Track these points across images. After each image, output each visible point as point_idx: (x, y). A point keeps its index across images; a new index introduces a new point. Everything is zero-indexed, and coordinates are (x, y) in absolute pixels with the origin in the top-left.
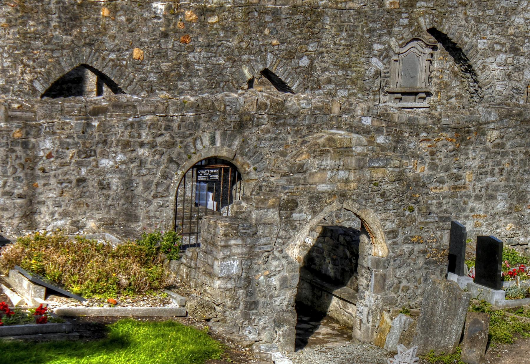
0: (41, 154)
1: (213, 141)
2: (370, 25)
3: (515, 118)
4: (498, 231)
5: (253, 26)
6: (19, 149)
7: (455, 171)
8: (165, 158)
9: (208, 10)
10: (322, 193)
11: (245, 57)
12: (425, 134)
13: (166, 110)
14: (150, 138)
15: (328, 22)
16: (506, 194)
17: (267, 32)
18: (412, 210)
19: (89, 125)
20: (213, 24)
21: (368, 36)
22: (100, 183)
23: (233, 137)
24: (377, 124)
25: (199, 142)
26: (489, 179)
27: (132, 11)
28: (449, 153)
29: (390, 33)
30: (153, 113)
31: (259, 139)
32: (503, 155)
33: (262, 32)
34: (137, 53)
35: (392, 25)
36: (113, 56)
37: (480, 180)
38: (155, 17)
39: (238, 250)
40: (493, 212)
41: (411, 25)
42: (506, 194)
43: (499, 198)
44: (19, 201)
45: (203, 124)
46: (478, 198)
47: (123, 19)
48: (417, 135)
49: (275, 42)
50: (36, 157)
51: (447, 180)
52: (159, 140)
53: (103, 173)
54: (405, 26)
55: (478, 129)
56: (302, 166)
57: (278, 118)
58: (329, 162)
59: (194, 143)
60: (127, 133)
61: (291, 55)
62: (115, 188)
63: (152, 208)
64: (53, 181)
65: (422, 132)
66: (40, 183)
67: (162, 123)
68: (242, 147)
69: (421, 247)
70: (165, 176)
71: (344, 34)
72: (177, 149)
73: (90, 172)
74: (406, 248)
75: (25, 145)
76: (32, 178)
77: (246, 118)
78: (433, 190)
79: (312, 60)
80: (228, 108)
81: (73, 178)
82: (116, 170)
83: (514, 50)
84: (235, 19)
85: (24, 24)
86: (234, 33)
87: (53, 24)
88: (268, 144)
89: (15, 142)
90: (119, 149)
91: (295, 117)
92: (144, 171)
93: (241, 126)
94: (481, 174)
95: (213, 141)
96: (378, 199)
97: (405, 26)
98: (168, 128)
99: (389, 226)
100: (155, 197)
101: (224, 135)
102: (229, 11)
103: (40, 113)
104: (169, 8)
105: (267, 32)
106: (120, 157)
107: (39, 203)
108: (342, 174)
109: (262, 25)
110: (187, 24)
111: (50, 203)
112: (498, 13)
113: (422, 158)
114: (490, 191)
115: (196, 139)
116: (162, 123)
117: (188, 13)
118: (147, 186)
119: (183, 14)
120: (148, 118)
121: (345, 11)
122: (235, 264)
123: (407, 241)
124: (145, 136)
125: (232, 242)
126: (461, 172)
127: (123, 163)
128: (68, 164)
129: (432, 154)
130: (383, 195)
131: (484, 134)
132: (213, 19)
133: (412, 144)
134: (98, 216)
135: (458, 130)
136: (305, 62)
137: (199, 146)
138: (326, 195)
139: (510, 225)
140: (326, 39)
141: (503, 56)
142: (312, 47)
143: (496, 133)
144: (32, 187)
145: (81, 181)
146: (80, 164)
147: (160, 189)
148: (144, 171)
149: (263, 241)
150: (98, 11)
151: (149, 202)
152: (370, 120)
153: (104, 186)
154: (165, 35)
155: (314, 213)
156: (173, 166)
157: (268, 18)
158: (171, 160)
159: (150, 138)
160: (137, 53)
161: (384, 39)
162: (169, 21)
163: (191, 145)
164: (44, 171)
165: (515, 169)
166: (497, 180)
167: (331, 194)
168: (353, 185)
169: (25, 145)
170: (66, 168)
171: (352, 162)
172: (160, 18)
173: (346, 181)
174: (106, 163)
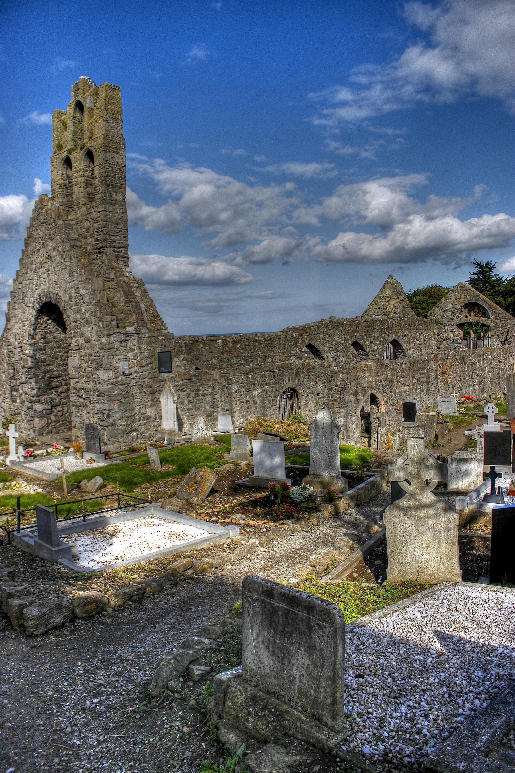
0: (233, 391)
1: (289, 382)
5: (252, 347)
6: (225, 389)
8: (274, 389)
11: (250, 360)
13: (273, 369)
14: (269, 382)
17: (257, 349)
18: (391, 392)
19: (248, 377)
22: (254, 402)
23: (295, 379)
24: (339, 369)
27: (211, 344)
29: (296, 346)
30: (269, 371)
31: (303, 379)
34: (214, 361)
35: (297, 343)
36: (206, 363)
39: (343, 414)
41: (302, 343)
44: (227, 412)
45: (286, 374)
47: (208, 348)
49: (260, 353)
50: (232, 392)
52: (272, 381)
53: (254, 397)
54: (300, 343)
56: (359, 376)
58: (366, 374)
60: (261, 380)
61: (265, 358)
63: (271, 411)
64: (238, 402)
66: (234, 403)
67: (272, 374)
68: (298, 382)
69: (395, 407)
70: (275, 397)
71: (281, 348)
72: (278, 385)
73: (250, 397)
74: (391, 408)
75: (227, 388)
76: (231, 402)
79: (272, 359)
81: (244, 401)
82: (258, 396)
83: (336, 350)
86: (246, 351)
87: (184, 352)
88: (306, 380)
89: (224, 387)
90: (259, 387)
91: (314, 369)
92: (268, 395)
93: (297, 374)
95: (289, 382)
96: (381, 389)
97: (300, 343)
98: (274, 376)
99: (385, 399)
100: (272, 406)
101: (292, 378)
103: (232, 373)
104: (223, 342)
105: (257, 349)
106: (260, 390)
107: (234, 412)
108: (371, 379)
109: (255, 347)
110: (230, 348)
111: (238, 412)
112: (329, 336)
116: (272, 374)
117: (230, 344)
118: (269, 401)
119: (228, 344)
120: (267, 373)
123: (391, 405)
125: (341, 410)
127: (261, 392)
128: (242, 395)
130: (382, 387)
132: (239, 345)
134: (254, 416)
136: (270, 360)
140: (276, 350)
141: (333, 352)
142: (272, 354)
144: (231, 406)
145: (247, 401)
146: (246, 395)
147: (274, 403)
148: (268, 395)
149: (350, 409)
150: (199, 345)
151: (270, 408)
153: (255, 403)
154: (223, 353)
155: (364, 396)
158: (276, 390)
159: (269, 382)
160: (214, 361)
161: (295, 349)
162: (223, 347)
164: (235, 398)
168: (374, 383)
169: (227, 388)
170: (242, 397)
174: (255, 393)
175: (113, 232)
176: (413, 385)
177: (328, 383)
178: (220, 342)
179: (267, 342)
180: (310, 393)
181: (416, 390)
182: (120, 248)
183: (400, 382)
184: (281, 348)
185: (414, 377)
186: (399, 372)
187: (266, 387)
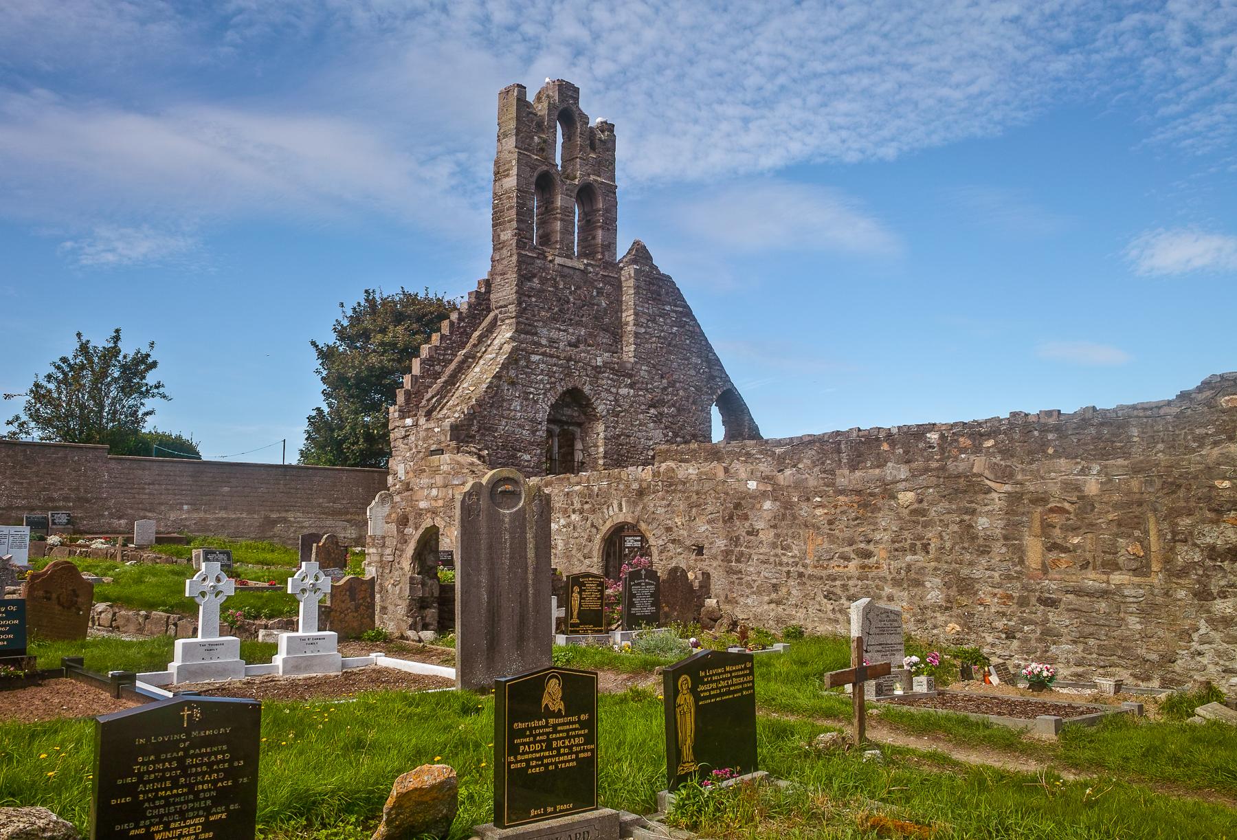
1: (621, 510)
2: (1197, 431)
3: (935, 473)
4: (935, 631)
7: (862, 545)
9: (981, 435)
10: (422, 510)
12: (819, 499)
15: (1136, 434)
16: (938, 580)
17: (1051, 451)
20: (989, 447)
21: (1195, 445)
23: (635, 504)
24: (762, 488)
25: (611, 508)
26: (909, 558)
28: (851, 522)
32: (925, 526)
33: (1044, 452)
37: (895, 558)
38: (930, 447)
40: (922, 604)
42: (938, 580)
43: (928, 584)
46: (897, 583)
47: (901, 451)
48: (808, 499)
51: (853, 556)
52: (586, 507)
55: (885, 489)
57: (671, 485)
59: (608, 509)
62: (560, 548)
65: (814, 497)
71: (1160, 446)
77: (644, 485)
78: (836, 568)
80: (630, 477)
84: (1012, 440)
85: (823, 463)
90: (561, 516)
91: (685, 483)
93: (641, 493)
94: (897, 550)
102: (1005, 433)
104: (942, 437)
105: (1051, 451)
108: (434, 492)
113: (819, 528)
114: (913, 575)
115: (609, 506)
117: (961, 439)
119: (956, 441)
121: (1159, 419)
122: (374, 569)
124: (577, 506)
126: (871, 547)
129: (830, 523)
131: (893, 497)
132: (990, 443)
133: (804, 510)
135: (859, 492)
137: (611, 513)
138: (424, 512)
139: (951, 625)
143: (910, 496)
148: (576, 535)
150: (879, 446)
152: (755, 483)
156: (594, 530)
157: (1050, 436)
158: (593, 525)
163: (605, 511)
165: (948, 545)
166: (919, 559)
167: (428, 510)
168: (440, 503)
171: (439, 480)
172: (934, 448)
173: (436, 499)
175: (499, 287)
176: (1176, 573)
177: (725, 522)
178: (933, 437)
179: (1093, 431)
180: (674, 541)
181: (1203, 595)
182: (506, 306)
183: (1065, 550)
184: (1160, 446)
185: (1178, 538)
186: (1061, 510)
187: (573, 517)
